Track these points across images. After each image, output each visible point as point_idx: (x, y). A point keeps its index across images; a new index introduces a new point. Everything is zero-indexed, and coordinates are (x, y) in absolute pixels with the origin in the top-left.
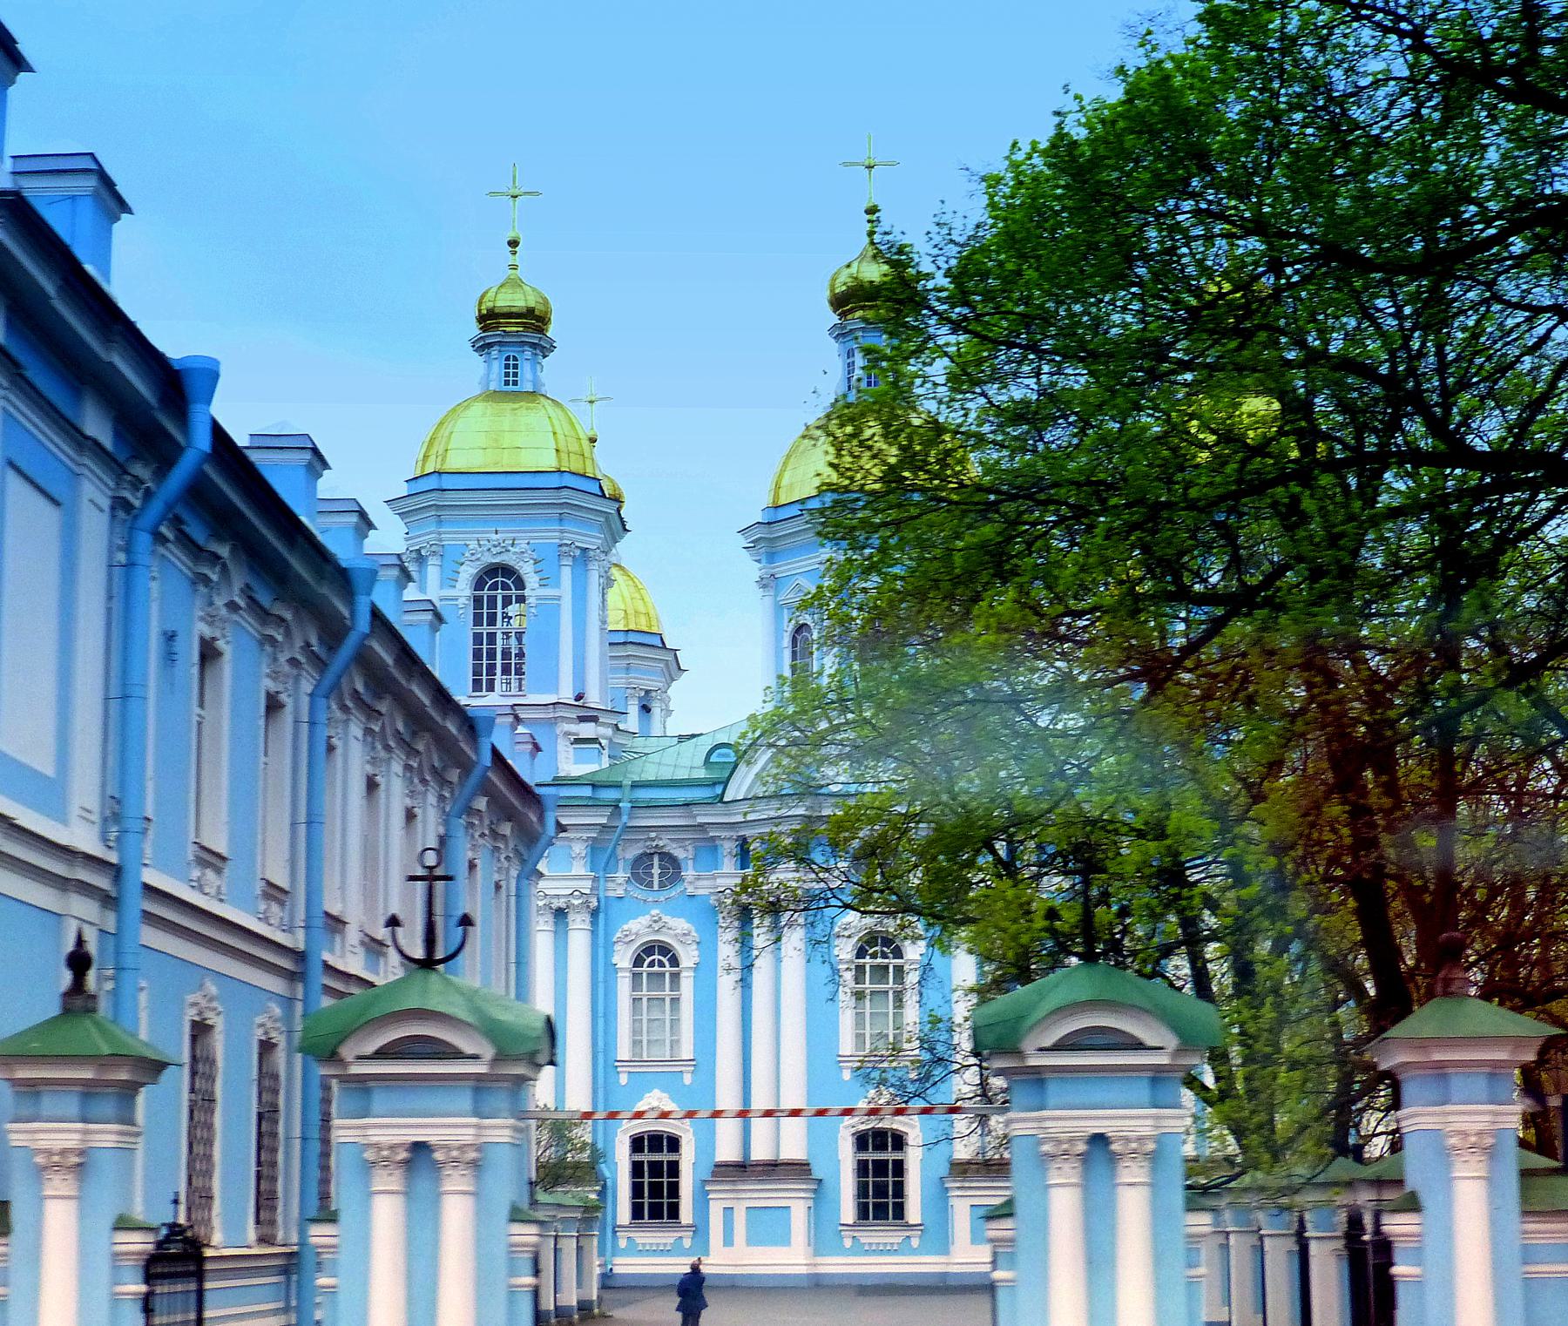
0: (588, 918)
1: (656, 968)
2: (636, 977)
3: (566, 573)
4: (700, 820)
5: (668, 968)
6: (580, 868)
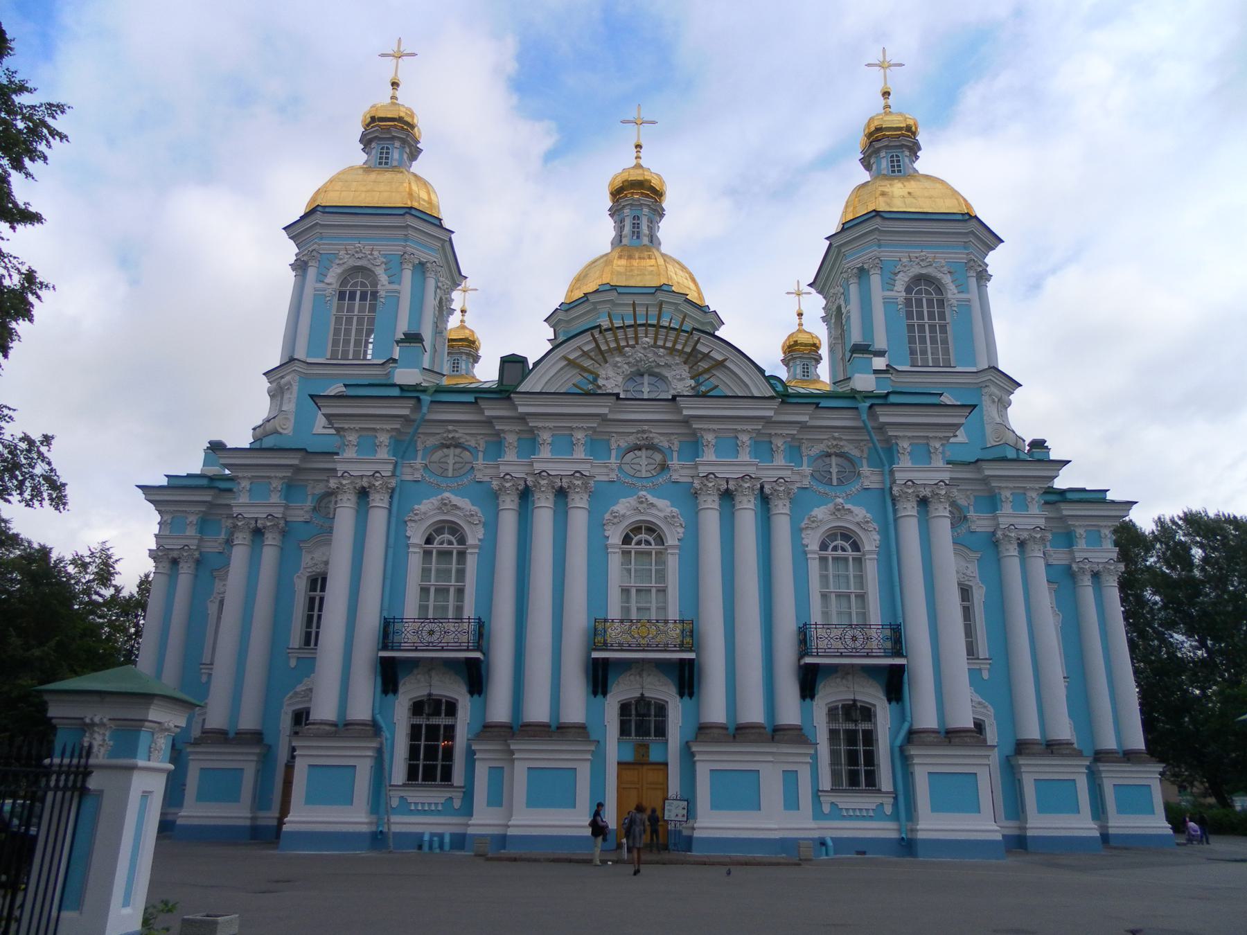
0: (387, 497)
1: (445, 545)
2: (427, 553)
3: (407, 275)
4: (487, 413)
5: (455, 545)
6: (383, 454)
